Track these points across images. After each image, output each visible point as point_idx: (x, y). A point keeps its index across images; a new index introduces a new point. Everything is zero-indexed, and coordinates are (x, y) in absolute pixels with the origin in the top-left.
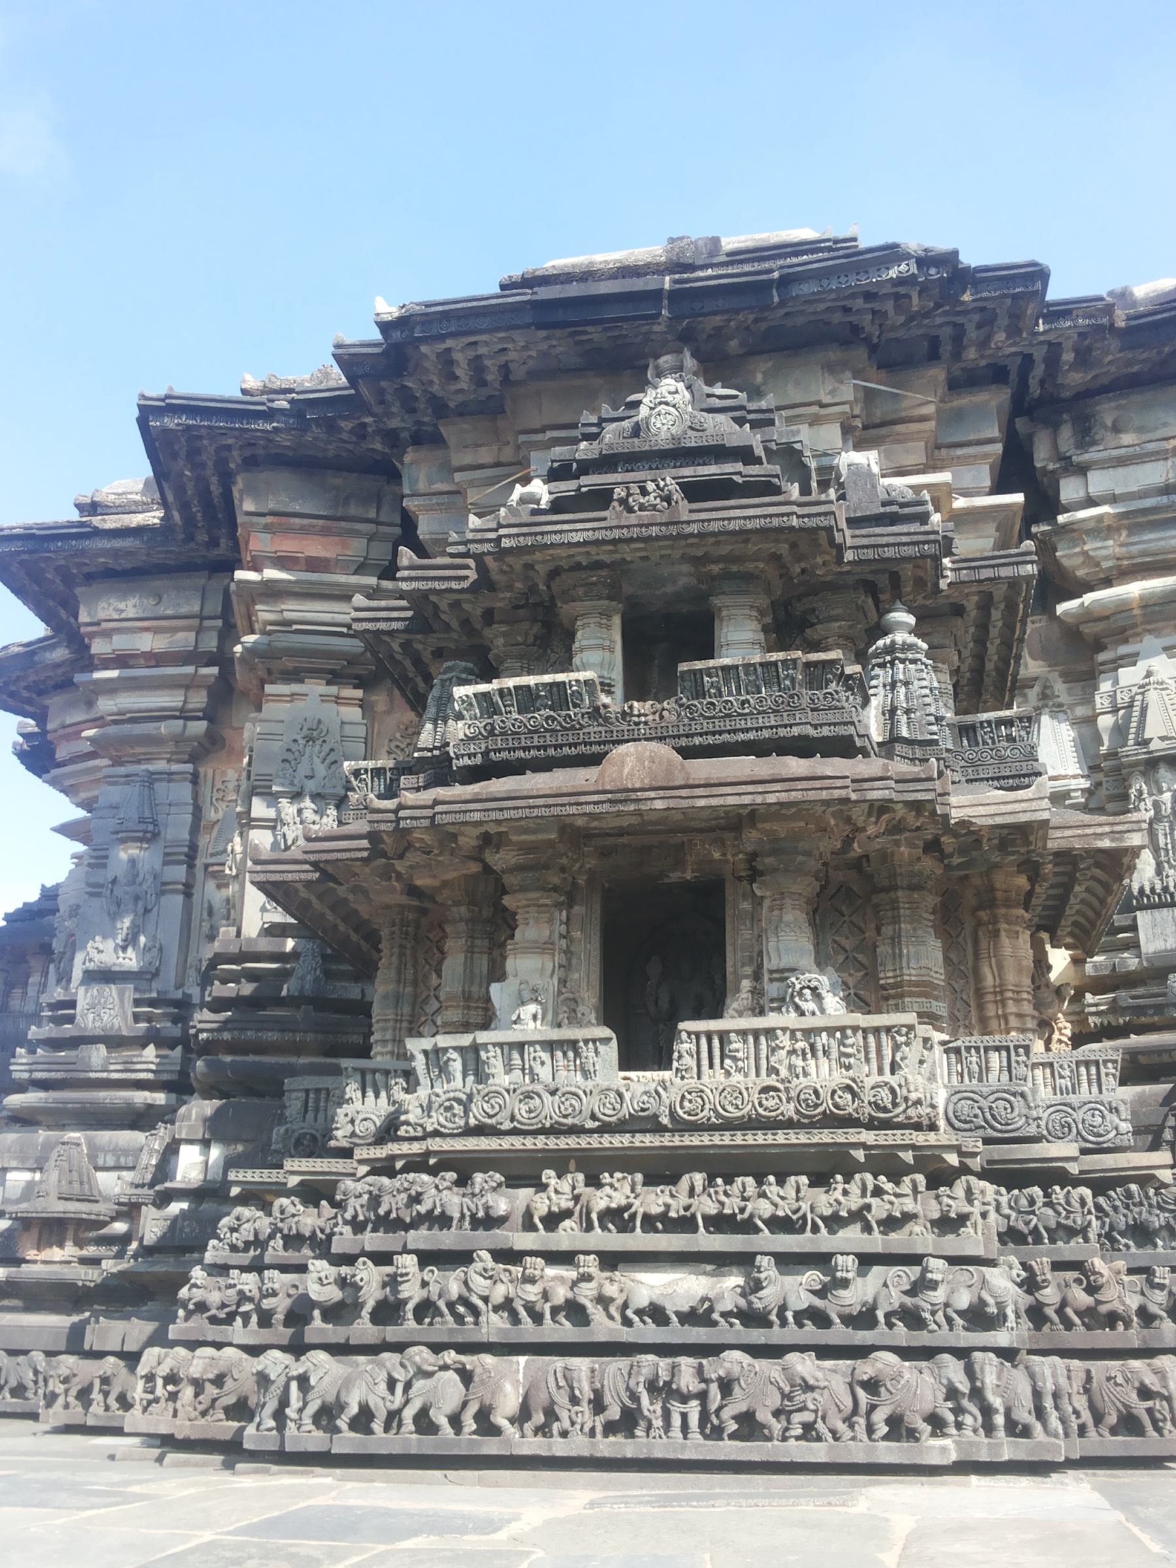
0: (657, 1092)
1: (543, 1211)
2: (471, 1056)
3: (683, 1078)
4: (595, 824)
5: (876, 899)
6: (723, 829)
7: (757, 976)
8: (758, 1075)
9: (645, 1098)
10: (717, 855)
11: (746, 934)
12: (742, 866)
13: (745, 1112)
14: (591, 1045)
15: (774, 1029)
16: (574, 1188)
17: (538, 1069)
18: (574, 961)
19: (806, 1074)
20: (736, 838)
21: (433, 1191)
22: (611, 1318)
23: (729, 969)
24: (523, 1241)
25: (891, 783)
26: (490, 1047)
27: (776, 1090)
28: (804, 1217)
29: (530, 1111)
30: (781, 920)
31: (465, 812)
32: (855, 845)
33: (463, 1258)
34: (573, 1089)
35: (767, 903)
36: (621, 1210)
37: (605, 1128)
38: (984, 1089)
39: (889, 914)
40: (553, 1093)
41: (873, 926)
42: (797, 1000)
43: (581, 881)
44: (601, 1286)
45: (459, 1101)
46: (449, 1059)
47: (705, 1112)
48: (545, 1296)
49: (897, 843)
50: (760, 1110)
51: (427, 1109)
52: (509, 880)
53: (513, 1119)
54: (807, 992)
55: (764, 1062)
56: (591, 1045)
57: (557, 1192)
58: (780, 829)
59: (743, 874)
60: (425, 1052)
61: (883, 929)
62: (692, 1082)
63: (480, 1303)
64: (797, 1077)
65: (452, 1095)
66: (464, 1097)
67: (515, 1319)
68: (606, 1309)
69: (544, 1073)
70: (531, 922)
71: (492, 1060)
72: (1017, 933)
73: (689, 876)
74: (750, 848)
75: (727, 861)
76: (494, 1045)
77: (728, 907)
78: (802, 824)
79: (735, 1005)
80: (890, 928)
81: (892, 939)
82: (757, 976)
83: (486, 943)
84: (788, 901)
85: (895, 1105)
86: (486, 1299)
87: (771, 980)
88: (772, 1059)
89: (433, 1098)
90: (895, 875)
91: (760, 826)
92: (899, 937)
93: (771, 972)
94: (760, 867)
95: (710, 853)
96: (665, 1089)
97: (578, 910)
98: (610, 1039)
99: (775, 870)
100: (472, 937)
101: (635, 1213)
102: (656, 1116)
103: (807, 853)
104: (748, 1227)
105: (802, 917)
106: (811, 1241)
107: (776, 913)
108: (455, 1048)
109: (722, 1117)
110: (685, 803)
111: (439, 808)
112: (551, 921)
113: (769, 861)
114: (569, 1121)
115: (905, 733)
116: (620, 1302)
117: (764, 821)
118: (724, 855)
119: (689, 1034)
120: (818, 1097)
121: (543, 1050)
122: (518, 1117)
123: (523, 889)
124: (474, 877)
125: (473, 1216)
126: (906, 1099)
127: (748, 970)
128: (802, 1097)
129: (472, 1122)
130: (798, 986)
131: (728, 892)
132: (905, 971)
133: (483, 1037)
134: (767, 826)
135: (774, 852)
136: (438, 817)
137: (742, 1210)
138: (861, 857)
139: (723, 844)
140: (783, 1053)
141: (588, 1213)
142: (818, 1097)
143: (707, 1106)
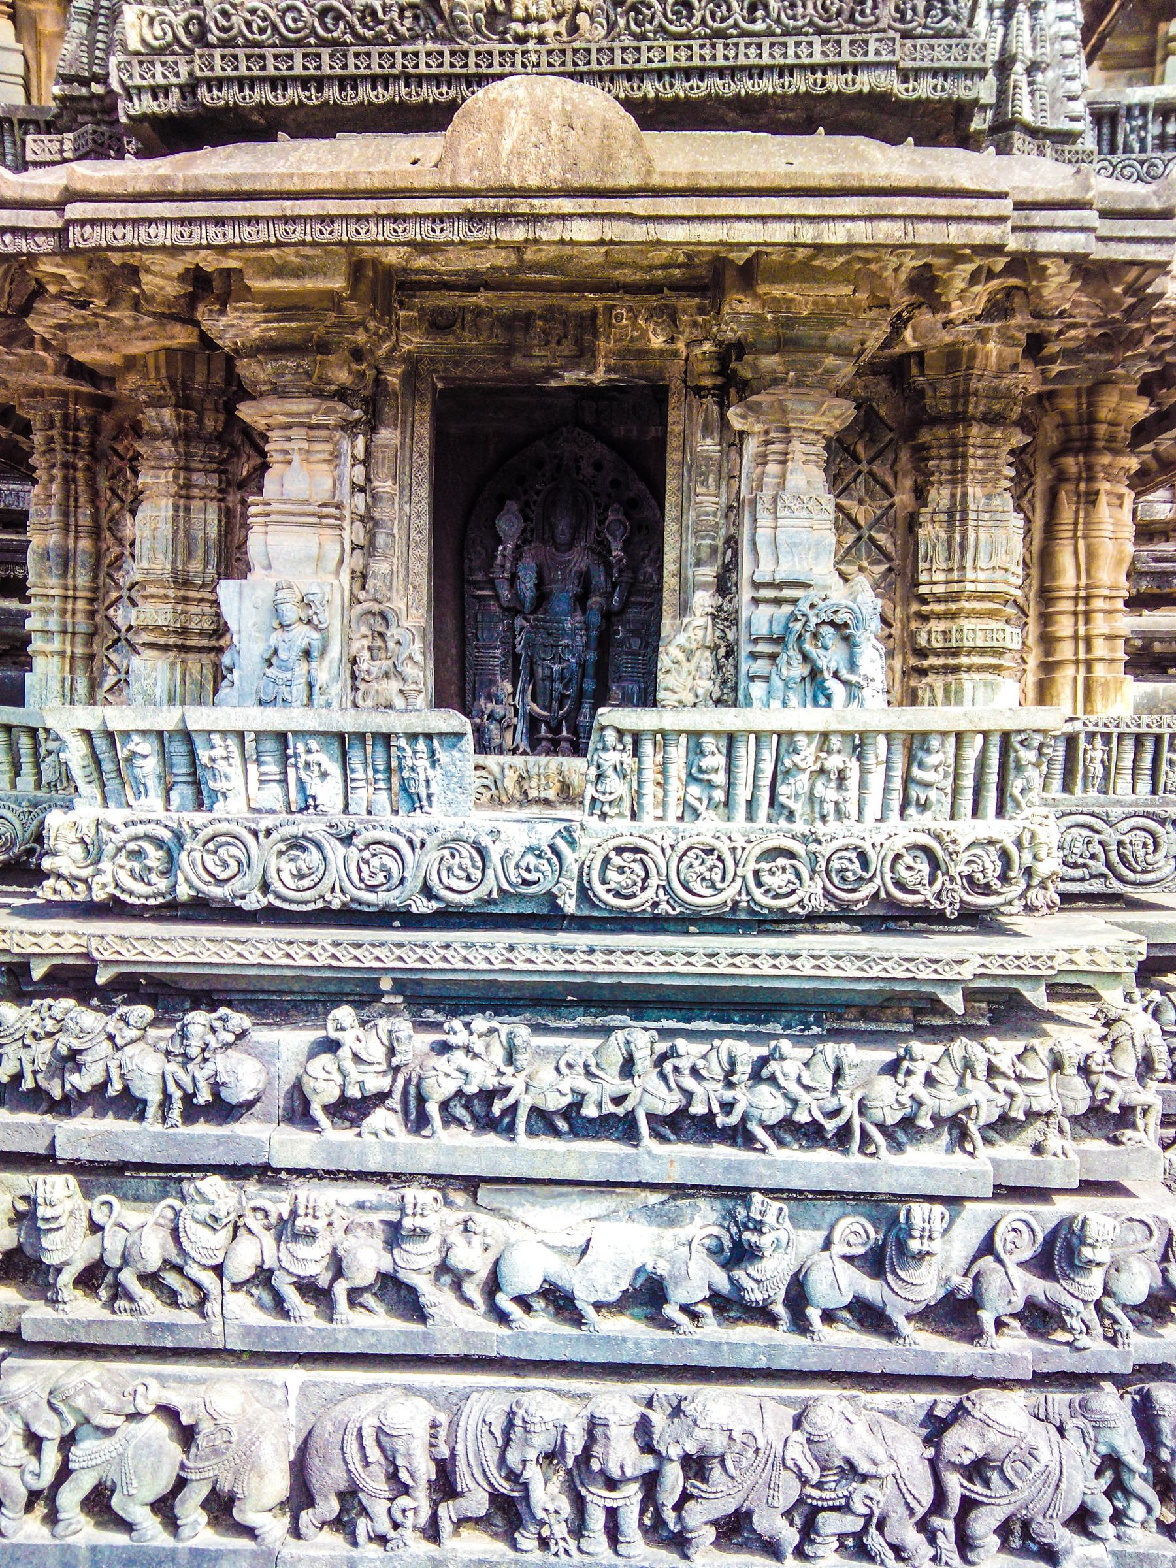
0: (552, 847)
1: (331, 1094)
2: (177, 748)
3: (603, 816)
4: (422, 262)
5: (925, 436)
6: (677, 287)
7: (724, 586)
8: (750, 818)
9: (531, 859)
10: (657, 342)
11: (709, 500)
12: (705, 367)
13: (729, 894)
14: (421, 745)
15: (791, 734)
16: (392, 1052)
17: (314, 786)
18: (381, 539)
19: (840, 814)
20: (701, 310)
21: (106, 1046)
22: (469, 1302)
23: (669, 567)
24: (291, 1146)
25: (1090, 217)
26: (216, 739)
27: (792, 855)
28: (848, 1126)
29: (301, 876)
30: (782, 483)
31: (136, 222)
32: (908, 333)
33: (172, 1175)
34: (386, 836)
35: (751, 447)
36: (488, 1096)
37: (449, 918)
38: (1116, 812)
39: (946, 465)
40: (347, 840)
41: (908, 483)
42: (807, 647)
43: (393, 379)
44: (447, 1248)
45: (159, 843)
46: (133, 754)
47: (650, 893)
48: (338, 1267)
49: (982, 336)
50: (758, 893)
51: (93, 852)
52: (251, 371)
53: (265, 887)
54: (827, 630)
55: (764, 794)
56: (421, 745)
57: (356, 1057)
58: (801, 297)
59: (707, 382)
60: (87, 734)
61: (933, 493)
62: (622, 828)
63: (208, 1279)
64: (823, 818)
65: (140, 829)
66: (166, 835)
67: (279, 1306)
68: (457, 1286)
69: (328, 793)
70: (296, 458)
71: (221, 765)
72: (1121, 497)
73: (599, 377)
74: (731, 332)
75: (675, 354)
76: (224, 733)
77: (673, 443)
78: (848, 290)
79: (681, 639)
80: (946, 492)
81: (951, 513)
82: (724, 586)
83: (213, 481)
84: (796, 446)
85: (1004, 878)
86: (219, 1270)
87: (756, 601)
88: (783, 790)
89: (105, 834)
90: (966, 394)
91: (762, 289)
92: (965, 511)
93: (756, 586)
94: (746, 373)
95: (644, 333)
96: (572, 843)
97: (387, 436)
98: (460, 736)
99: (776, 381)
100: (187, 469)
101: (515, 1106)
102: (551, 897)
103: (842, 351)
104: (740, 1136)
105: (818, 477)
106: (861, 1170)
107: (773, 468)
108: (144, 733)
109: (682, 903)
110: (639, 233)
111: (75, 210)
112: (335, 457)
113: (769, 362)
114: (380, 898)
115: (1027, 116)
116: (483, 1274)
117: (774, 279)
118: (672, 340)
119: (621, 733)
120: (865, 865)
121: (323, 748)
122: (276, 885)
123: (278, 391)
124: (187, 353)
125: (188, 1098)
126: (1028, 872)
127: (708, 573)
128: (836, 864)
129: (184, 892)
130: (814, 620)
131: (674, 415)
132: (970, 575)
133: (199, 718)
134: (777, 291)
135: (780, 345)
136: (74, 233)
137: (727, 1107)
138: (910, 355)
139: (673, 319)
140: (804, 777)
141: (422, 1100)
142: (865, 865)
143: (654, 881)
